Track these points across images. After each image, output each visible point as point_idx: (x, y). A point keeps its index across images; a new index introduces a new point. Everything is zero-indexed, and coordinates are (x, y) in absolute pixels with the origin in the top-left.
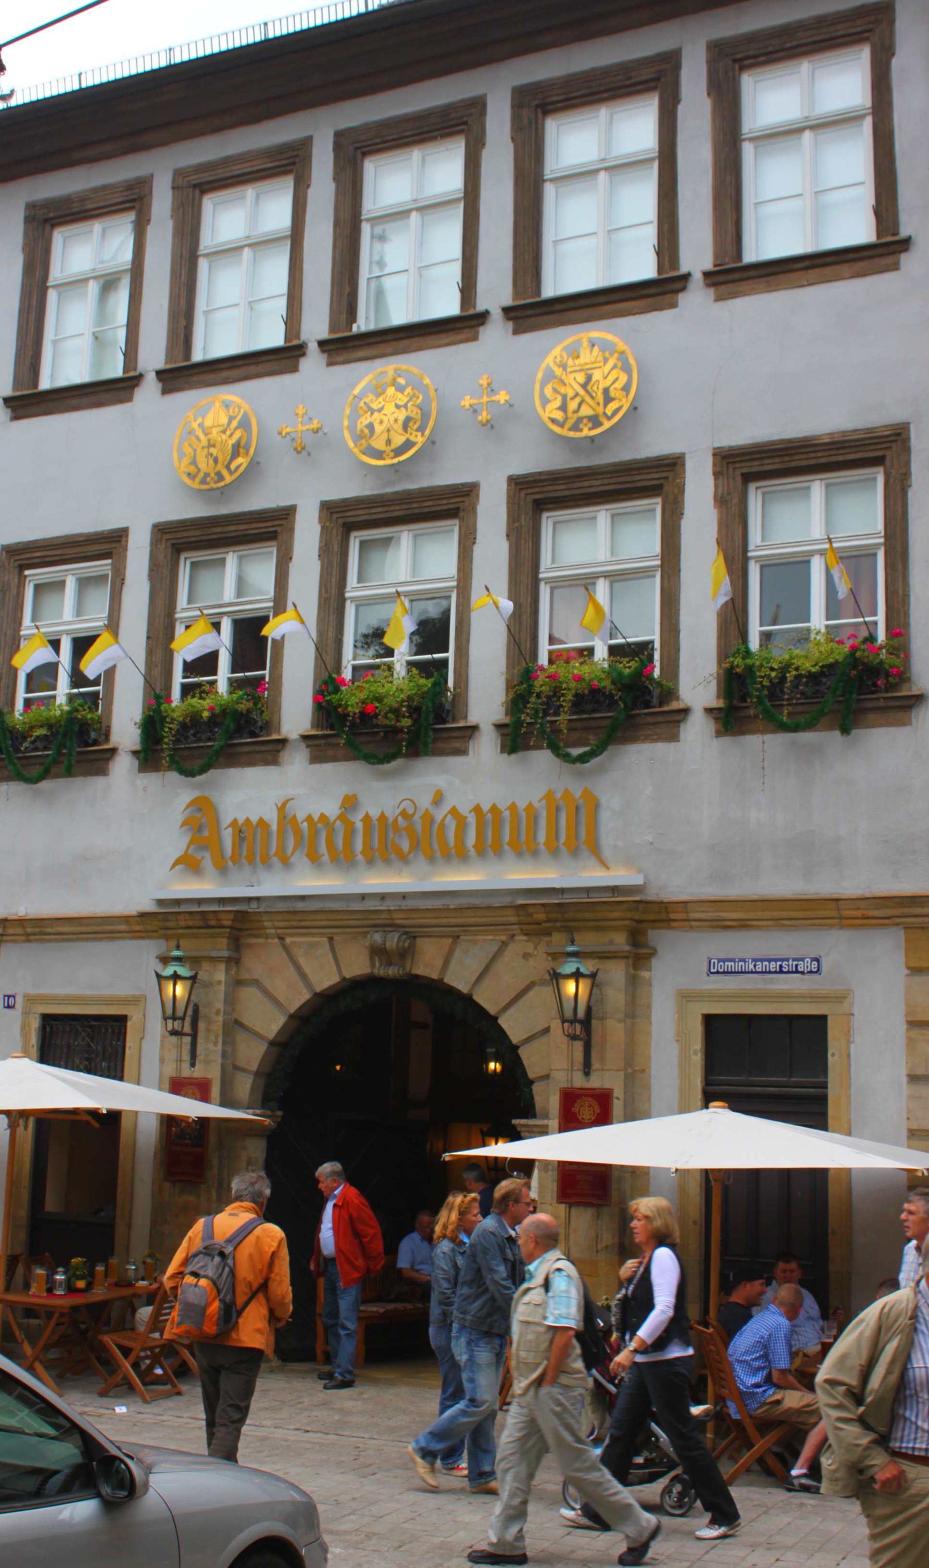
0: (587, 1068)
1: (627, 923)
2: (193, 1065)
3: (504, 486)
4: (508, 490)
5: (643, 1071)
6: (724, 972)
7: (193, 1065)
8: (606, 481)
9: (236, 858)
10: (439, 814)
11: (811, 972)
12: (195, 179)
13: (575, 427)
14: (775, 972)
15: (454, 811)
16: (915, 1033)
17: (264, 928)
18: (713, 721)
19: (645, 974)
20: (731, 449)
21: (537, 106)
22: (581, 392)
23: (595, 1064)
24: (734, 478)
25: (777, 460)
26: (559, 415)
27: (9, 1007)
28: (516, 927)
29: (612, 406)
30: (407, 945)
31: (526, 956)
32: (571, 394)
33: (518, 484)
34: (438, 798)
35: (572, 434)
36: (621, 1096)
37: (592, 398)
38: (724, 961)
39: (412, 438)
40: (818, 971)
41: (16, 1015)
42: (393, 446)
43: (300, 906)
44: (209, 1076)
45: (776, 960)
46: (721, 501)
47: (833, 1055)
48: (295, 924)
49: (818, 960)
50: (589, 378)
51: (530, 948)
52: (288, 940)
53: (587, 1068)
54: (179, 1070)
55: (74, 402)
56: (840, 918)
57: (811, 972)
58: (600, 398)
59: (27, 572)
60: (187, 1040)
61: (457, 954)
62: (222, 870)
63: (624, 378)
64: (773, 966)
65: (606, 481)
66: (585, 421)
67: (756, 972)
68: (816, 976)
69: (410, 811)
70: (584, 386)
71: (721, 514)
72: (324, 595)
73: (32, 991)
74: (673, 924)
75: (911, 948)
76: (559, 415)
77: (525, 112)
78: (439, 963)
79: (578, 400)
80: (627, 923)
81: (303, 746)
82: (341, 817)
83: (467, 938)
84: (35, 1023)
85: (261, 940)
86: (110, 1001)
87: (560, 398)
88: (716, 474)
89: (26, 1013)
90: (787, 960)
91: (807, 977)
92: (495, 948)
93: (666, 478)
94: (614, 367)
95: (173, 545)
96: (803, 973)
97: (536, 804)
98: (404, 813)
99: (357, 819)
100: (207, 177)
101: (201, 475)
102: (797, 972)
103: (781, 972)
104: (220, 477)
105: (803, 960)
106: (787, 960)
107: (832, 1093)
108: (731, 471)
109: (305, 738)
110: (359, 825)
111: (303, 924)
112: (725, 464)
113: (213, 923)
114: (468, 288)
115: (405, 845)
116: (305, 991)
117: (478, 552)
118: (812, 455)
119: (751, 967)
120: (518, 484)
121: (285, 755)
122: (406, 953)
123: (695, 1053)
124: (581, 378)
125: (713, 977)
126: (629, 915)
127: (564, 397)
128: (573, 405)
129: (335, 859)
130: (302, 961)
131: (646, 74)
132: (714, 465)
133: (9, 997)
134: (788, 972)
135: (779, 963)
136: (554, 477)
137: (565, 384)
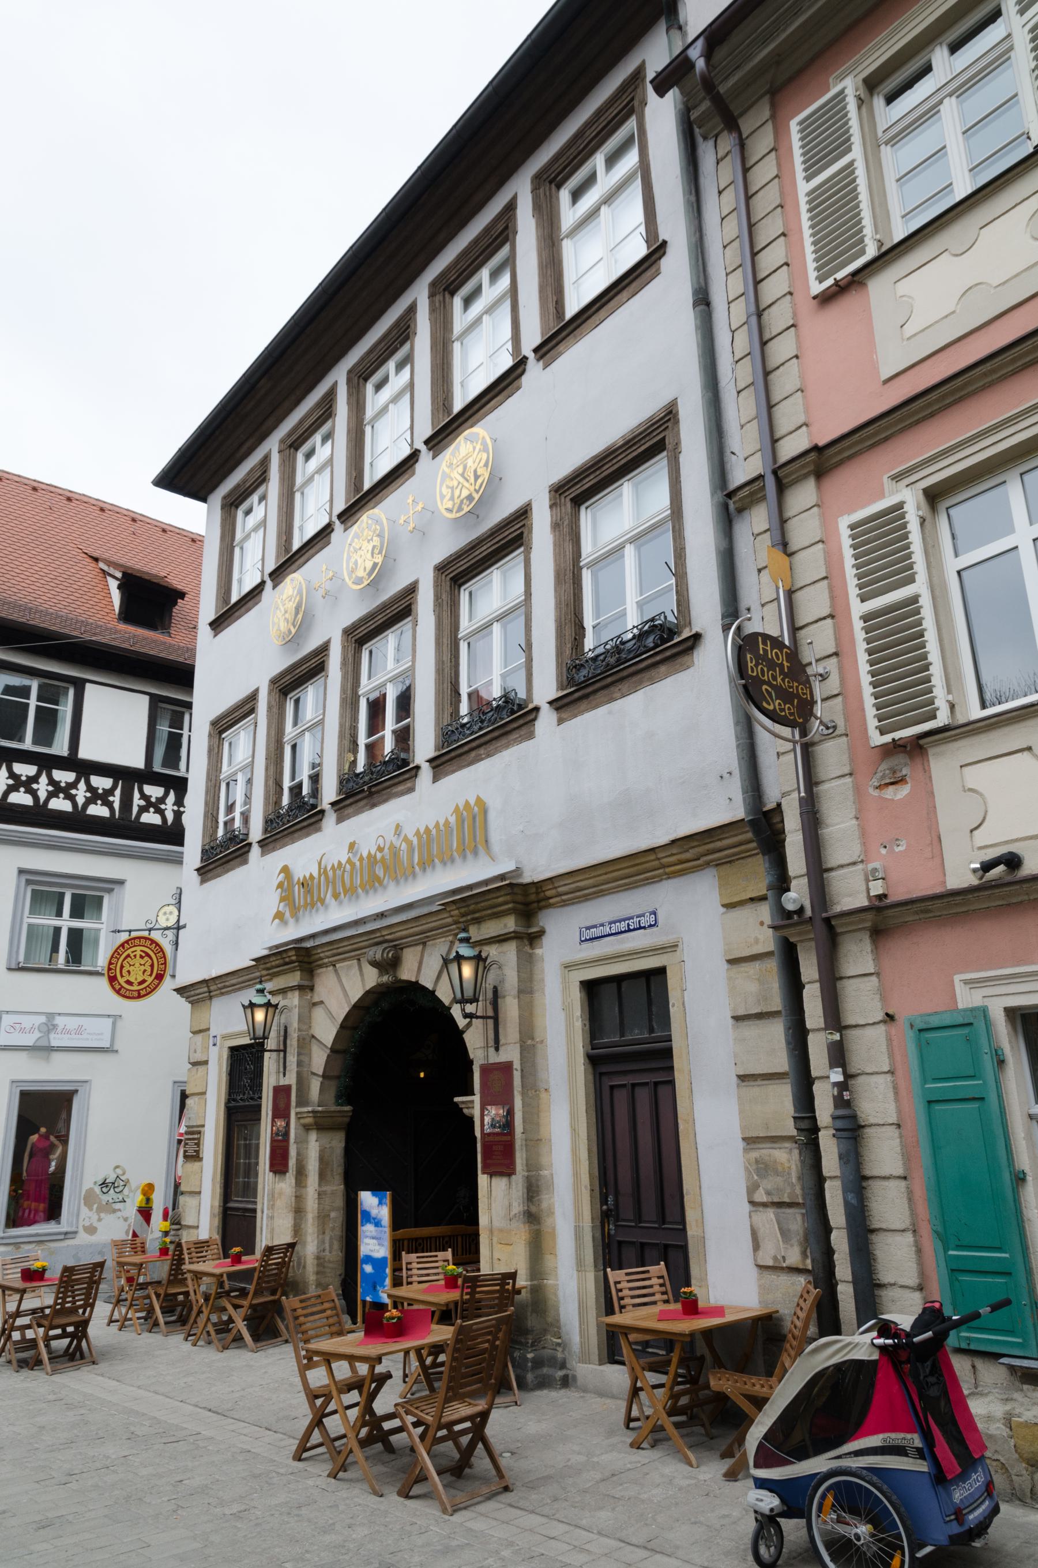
1: (510, 906)
4: (434, 577)
5: (542, 1042)
6: (590, 939)
7: (284, 1075)
8: (489, 545)
10: (397, 844)
11: (651, 926)
12: (289, 442)
13: (460, 509)
14: (625, 932)
15: (406, 839)
17: (321, 959)
18: (555, 713)
21: (444, 290)
22: (461, 480)
23: (502, 1041)
24: (565, 505)
25: (592, 477)
28: (454, 926)
29: (480, 481)
30: (390, 955)
32: (455, 483)
34: (398, 828)
35: (458, 515)
36: (519, 1068)
37: (467, 481)
38: (588, 928)
39: (377, 561)
42: (367, 571)
45: (624, 920)
46: (556, 526)
47: (673, 1005)
48: (335, 951)
49: (655, 913)
52: (337, 966)
54: (278, 1080)
55: (237, 614)
56: (664, 866)
57: (651, 926)
58: (472, 480)
60: (282, 1054)
63: (485, 456)
64: (623, 926)
65: (489, 545)
66: (465, 501)
67: (612, 934)
68: (655, 929)
69: (382, 846)
72: (344, 696)
73: (225, 1032)
74: (552, 901)
75: (723, 884)
76: (450, 505)
77: (438, 298)
79: (460, 486)
80: (510, 906)
82: (349, 861)
83: (431, 942)
85: (324, 969)
87: (450, 490)
90: (632, 918)
91: (648, 931)
93: (524, 525)
94: (480, 450)
95: (280, 690)
96: (644, 928)
98: (380, 849)
100: (294, 437)
102: (640, 928)
103: (629, 930)
104: (290, 631)
105: (643, 915)
106: (632, 918)
107: (677, 1045)
108: (563, 500)
110: (358, 864)
111: (340, 950)
112: (558, 496)
113: (287, 960)
116: (346, 1005)
118: (615, 461)
119: (608, 929)
122: (390, 965)
123: (577, 1020)
124: (460, 469)
125: (585, 945)
126: (508, 898)
128: (457, 493)
132: (550, 500)
134: (634, 930)
135: (627, 922)
137: (452, 480)
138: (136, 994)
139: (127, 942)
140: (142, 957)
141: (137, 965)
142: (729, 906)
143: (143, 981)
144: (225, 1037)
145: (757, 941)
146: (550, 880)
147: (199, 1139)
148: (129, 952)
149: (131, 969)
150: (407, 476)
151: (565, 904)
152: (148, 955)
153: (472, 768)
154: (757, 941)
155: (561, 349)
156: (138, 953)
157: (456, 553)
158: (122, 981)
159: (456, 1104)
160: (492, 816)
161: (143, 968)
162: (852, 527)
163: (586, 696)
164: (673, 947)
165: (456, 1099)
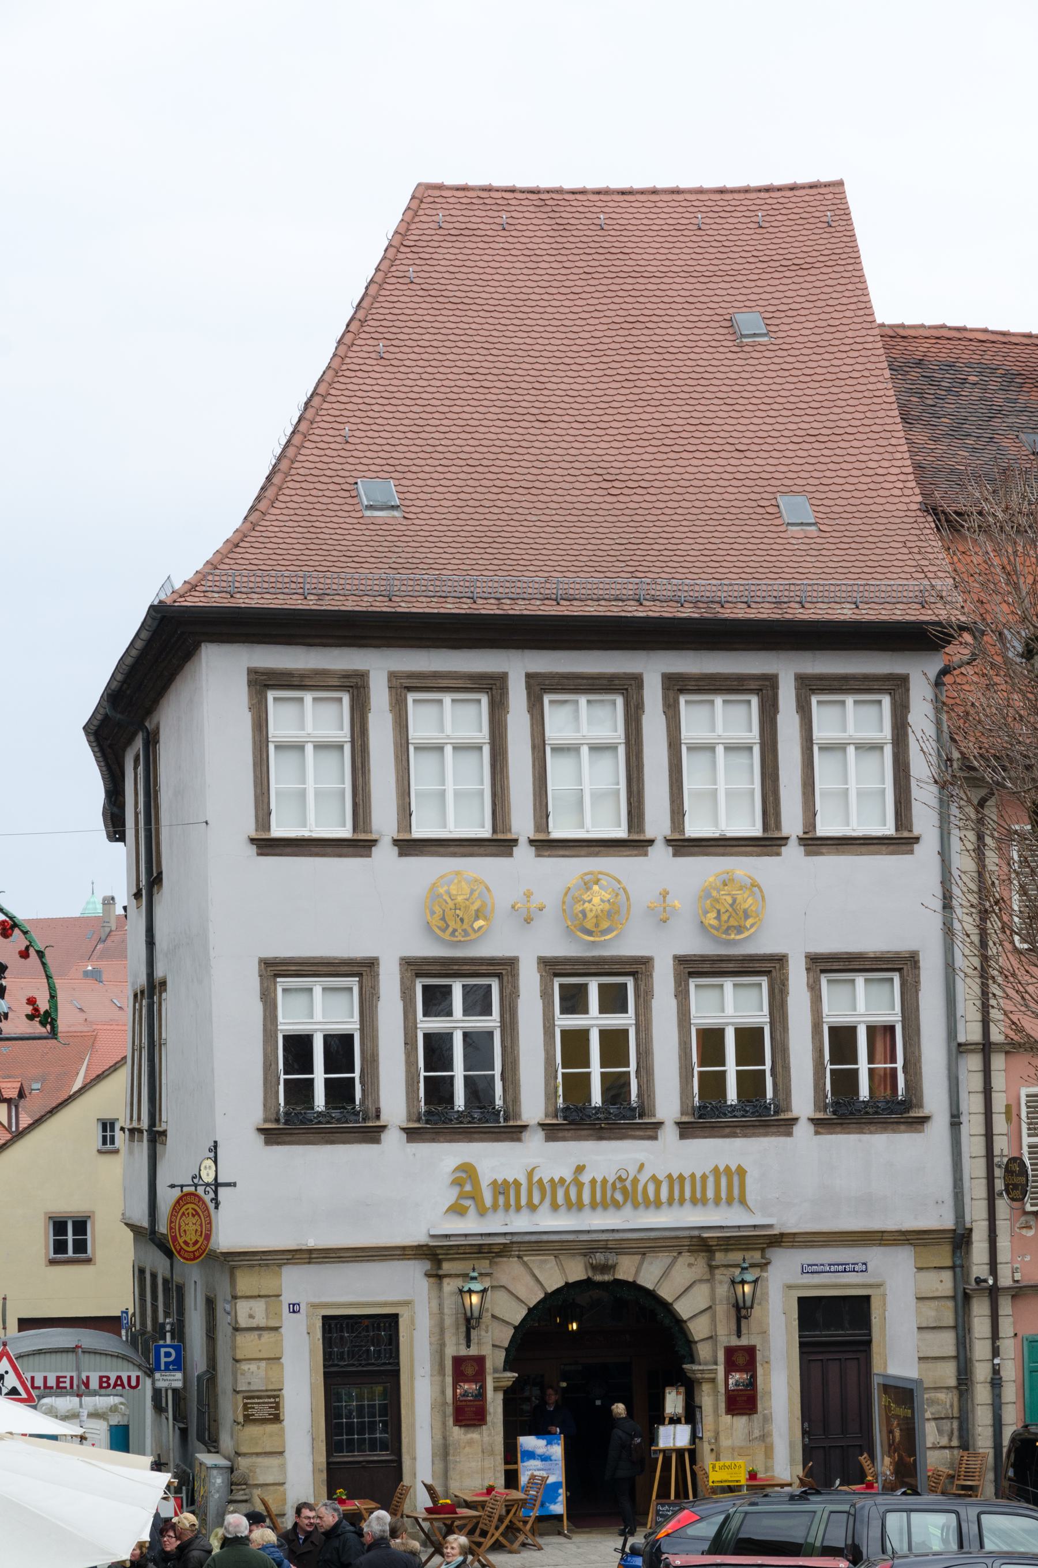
0: (739, 1334)
2: (468, 1346)
3: (671, 962)
7: (468, 1346)
9: (495, 1207)
15: (654, 1178)
16: (921, 1304)
19: (765, 1274)
20: (816, 954)
22: (730, 910)
23: (744, 1330)
26: (714, 922)
27: (294, 1312)
31: (690, 1265)
33: (681, 961)
38: (811, 1265)
40: (866, 1271)
41: (301, 1317)
43: (545, 1238)
44: (483, 1353)
50: (734, 901)
51: (692, 1260)
53: (739, 1334)
54: (458, 1350)
59: (279, 980)
62: (482, 1212)
64: (841, 1268)
69: (624, 1177)
70: (732, 905)
71: (812, 995)
72: (548, 1025)
76: (714, 922)
78: (633, 1270)
79: (727, 914)
81: (540, 1129)
84: (319, 1324)
85: (505, 1259)
86: (385, 1304)
88: (808, 970)
92: (670, 1260)
97: (707, 1173)
98: (620, 1178)
101: (450, 930)
109: (542, 1125)
114: (636, 814)
115: (619, 1197)
117: (656, 1004)
120: (681, 961)
121: (525, 1135)
127: (719, 911)
128: (725, 917)
130: (537, 1272)
131: (753, 685)
133: (294, 1305)
136: (704, 959)
138: (192, 1256)
139: (181, 1198)
140: (193, 1216)
141: (191, 1224)
142: (920, 1269)
143: (196, 1242)
144: (314, 1306)
145: (937, 1290)
146: (795, 1234)
147: (278, 1403)
148: (183, 1209)
149: (187, 1228)
150: (635, 852)
151: (793, 1247)
152: (197, 1213)
153: (727, 1140)
154: (937, 1290)
155: (824, 851)
156: (191, 1211)
157: (702, 956)
158: (181, 1241)
159: (683, 1369)
160: (749, 1180)
161: (194, 1227)
162: (1028, 1096)
163: (841, 1124)
164: (879, 1286)
165: (684, 1366)
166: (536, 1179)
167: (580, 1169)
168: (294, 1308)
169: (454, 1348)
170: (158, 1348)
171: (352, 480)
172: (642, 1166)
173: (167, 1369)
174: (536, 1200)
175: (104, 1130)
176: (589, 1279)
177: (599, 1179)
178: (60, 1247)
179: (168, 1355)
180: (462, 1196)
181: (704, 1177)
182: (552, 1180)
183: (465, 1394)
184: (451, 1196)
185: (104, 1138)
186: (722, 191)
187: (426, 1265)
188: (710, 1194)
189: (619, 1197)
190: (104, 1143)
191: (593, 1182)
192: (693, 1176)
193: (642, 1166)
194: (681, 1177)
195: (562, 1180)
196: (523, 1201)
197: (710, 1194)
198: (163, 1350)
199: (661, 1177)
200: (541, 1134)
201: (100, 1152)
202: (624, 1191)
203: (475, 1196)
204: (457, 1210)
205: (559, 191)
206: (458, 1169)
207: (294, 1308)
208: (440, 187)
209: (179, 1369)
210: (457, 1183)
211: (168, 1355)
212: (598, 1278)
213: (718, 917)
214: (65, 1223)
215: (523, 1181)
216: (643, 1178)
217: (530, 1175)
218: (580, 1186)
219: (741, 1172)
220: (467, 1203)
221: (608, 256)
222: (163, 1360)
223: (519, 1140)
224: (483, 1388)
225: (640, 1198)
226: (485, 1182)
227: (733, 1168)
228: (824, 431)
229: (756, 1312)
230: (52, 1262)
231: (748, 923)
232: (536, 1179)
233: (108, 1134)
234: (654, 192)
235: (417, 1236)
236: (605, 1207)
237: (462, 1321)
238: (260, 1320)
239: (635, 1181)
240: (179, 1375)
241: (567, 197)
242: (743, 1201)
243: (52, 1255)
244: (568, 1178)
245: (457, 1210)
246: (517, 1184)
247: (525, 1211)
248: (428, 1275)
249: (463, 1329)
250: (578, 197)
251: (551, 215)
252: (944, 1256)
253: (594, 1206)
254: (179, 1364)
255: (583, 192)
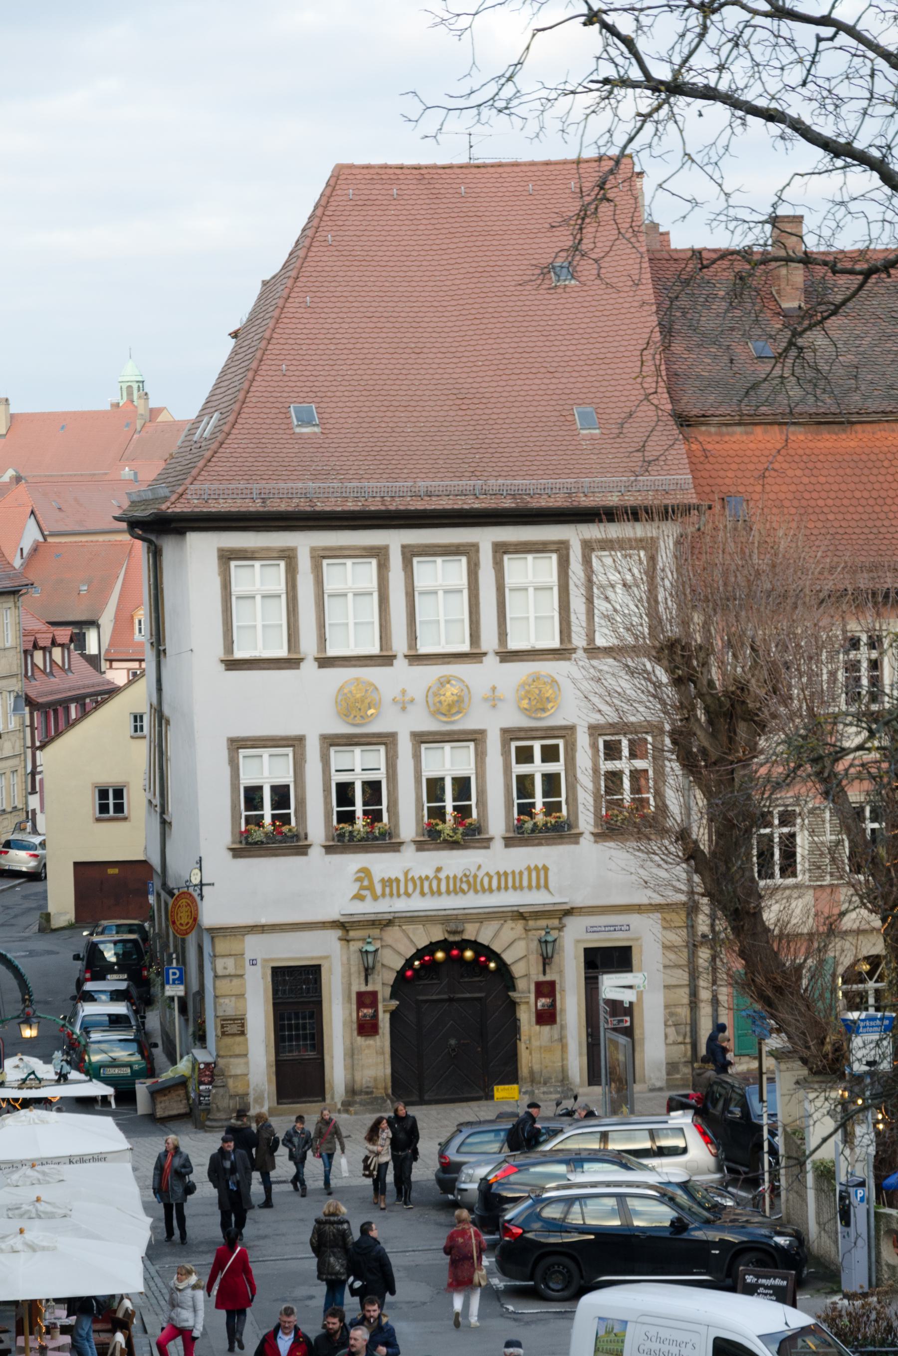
0: (544, 973)
9: (383, 895)
15: (487, 874)
23: (548, 971)
33: (504, 731)
41: (258, 968)
43: (416, 914)
51: (513, 925)
53: (544, 973)
61: (483, 929)
62: (375, 898)
77: (498, 555)
84: (269, 972)
86: (312, 958)
89: (263, 967)
98: (465, 875)
99: (442, 875)
109: (415, 842)
114: (475, 636)
115: (465, 887)
117: (488, 760)
120: (504, 731)
121: (403, 848)
129: (432, 893)
131: (554, 547)
136: (520, 730)
144: (265, 961)
160: (550, 874)
164: (637, 939)
166: (410, 876)
167: (439, 870)
168: (253, 963)
169: (358, 985)
170: (168, 970)
171: (287, 405)
172: (479, 867)
173: (174, 983)
174: (410, 890)
175: (136, 721)
176: (446, 940)
177: (451, 876)
178: (104, 808)
179: (174, 974)
180: (362, 888)
181: (521, 873)
182: (420, 878)
183: (365, 1015)
184: (354, 888)
185: (136, 727)
186: (547, 163)
187: (339, 933)
188: (525, 883)
189: (465, 887)
190: (136, 731)
191: (448, 878)
192: (513, 872)
193: (479, 867)
194: (506, 874)
195: (427, 878)
196: (402, 891)
197: (525, 883)
198: (171, 971)
199: (492, 873)
200: (413, 847)
201: (132, 737)
202: (468, 882)
203: (371, 888)
204: (359, 897)
205: (435, 167)
206: (360, 871)
207: (253, 963)
208: (351, 166)
209: (181, 983)
210: (358, 880)
211: (174, 974)
212: (452, 938)
213: (529, 703)
214: (107, 791)
215: (402, 878)
216: (481, 874)
217: (406, 874)
218: (439, 880)
219: (546, 868)
220: (364, 892)
221: (466, 219)
222: (171, 977)
223: (398, 851)
224: (376, 1011)
225: (479, 888)
226: (376, 879)
227: (540, 866)
228: (609, 355)
229: (556, 958)
230: (98, 820)
231: (550, 706)
232: (410, 876)
233: (138, 724)
234: (500, 165)
235: (333, 914)
236: (456, 893)
237: (362, 969)
238: (231, 970)
239: (475, 876)
240: (182, 987)
241: (440, 171)
242: (546, 887)
243: (98, 815)
244: (431, 874)
245: (359, 897)
246: (397, 880)
247: (403, 897)
248: (340, 939)
249: (363, 974)
250: (447, 171)
251: (428, 186)
252: (679, 919)
253: (448, 892)
254: (181, 980)
255: (450, 167)
